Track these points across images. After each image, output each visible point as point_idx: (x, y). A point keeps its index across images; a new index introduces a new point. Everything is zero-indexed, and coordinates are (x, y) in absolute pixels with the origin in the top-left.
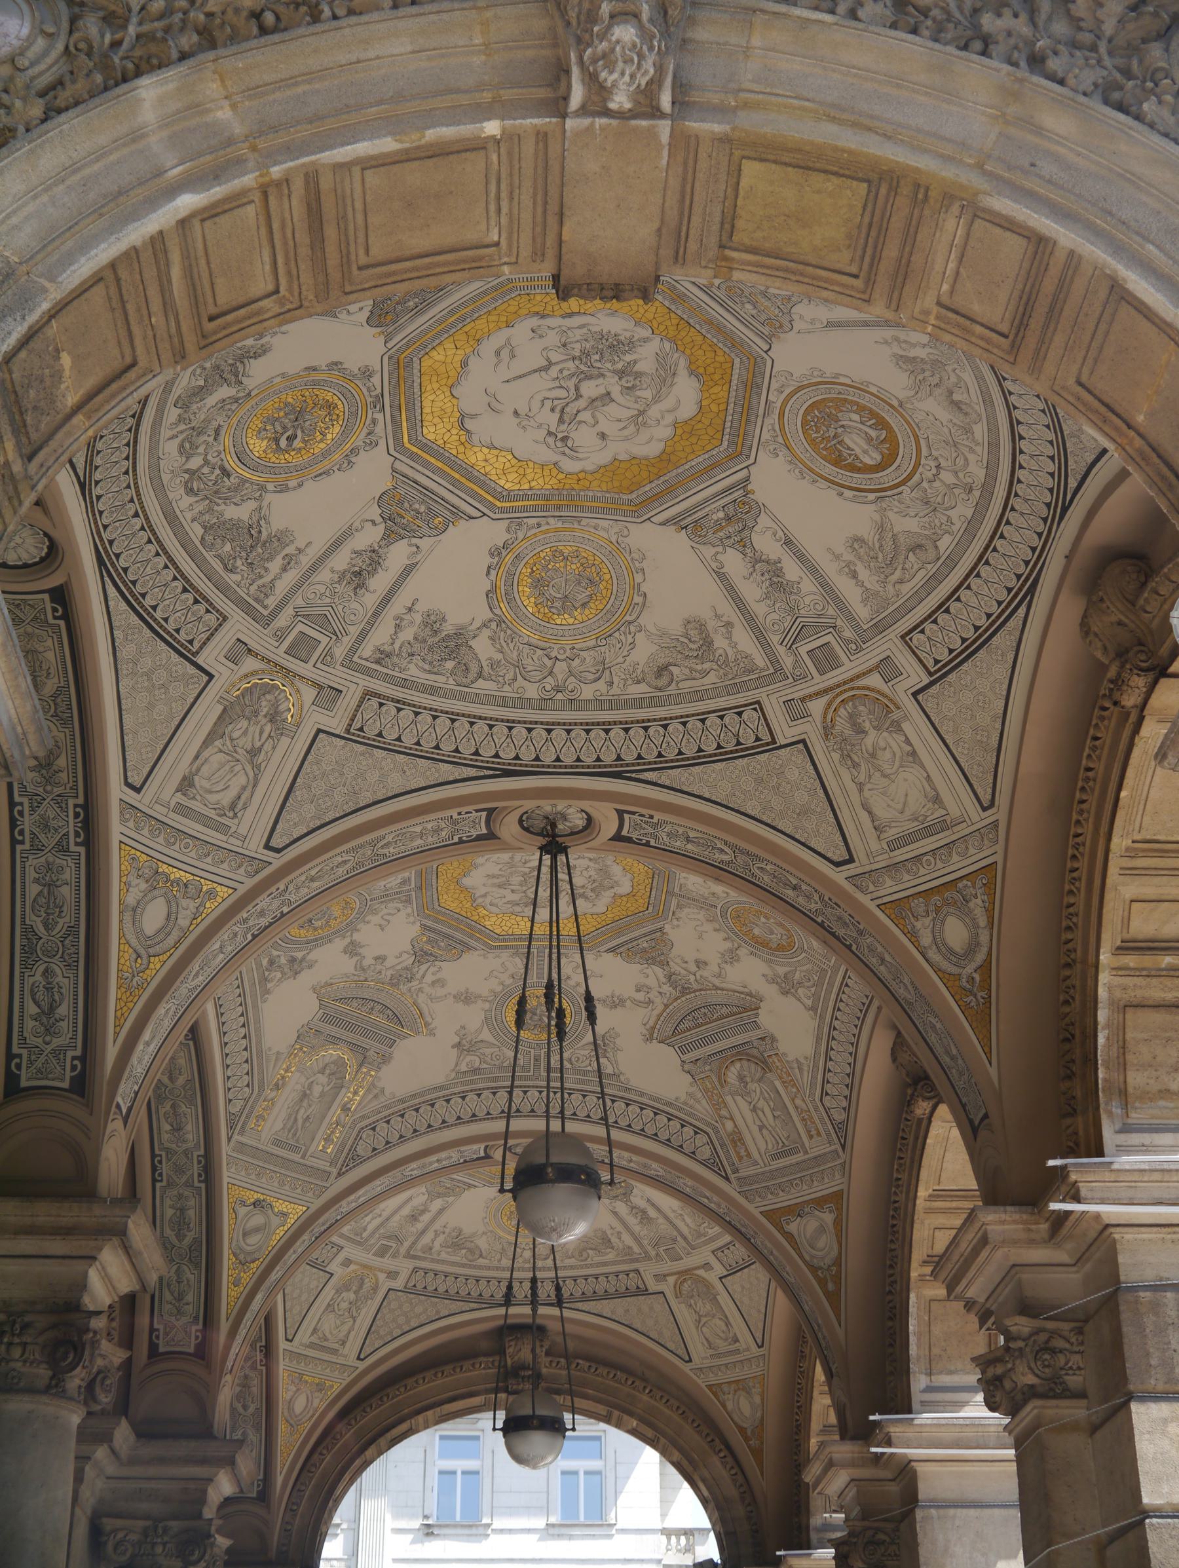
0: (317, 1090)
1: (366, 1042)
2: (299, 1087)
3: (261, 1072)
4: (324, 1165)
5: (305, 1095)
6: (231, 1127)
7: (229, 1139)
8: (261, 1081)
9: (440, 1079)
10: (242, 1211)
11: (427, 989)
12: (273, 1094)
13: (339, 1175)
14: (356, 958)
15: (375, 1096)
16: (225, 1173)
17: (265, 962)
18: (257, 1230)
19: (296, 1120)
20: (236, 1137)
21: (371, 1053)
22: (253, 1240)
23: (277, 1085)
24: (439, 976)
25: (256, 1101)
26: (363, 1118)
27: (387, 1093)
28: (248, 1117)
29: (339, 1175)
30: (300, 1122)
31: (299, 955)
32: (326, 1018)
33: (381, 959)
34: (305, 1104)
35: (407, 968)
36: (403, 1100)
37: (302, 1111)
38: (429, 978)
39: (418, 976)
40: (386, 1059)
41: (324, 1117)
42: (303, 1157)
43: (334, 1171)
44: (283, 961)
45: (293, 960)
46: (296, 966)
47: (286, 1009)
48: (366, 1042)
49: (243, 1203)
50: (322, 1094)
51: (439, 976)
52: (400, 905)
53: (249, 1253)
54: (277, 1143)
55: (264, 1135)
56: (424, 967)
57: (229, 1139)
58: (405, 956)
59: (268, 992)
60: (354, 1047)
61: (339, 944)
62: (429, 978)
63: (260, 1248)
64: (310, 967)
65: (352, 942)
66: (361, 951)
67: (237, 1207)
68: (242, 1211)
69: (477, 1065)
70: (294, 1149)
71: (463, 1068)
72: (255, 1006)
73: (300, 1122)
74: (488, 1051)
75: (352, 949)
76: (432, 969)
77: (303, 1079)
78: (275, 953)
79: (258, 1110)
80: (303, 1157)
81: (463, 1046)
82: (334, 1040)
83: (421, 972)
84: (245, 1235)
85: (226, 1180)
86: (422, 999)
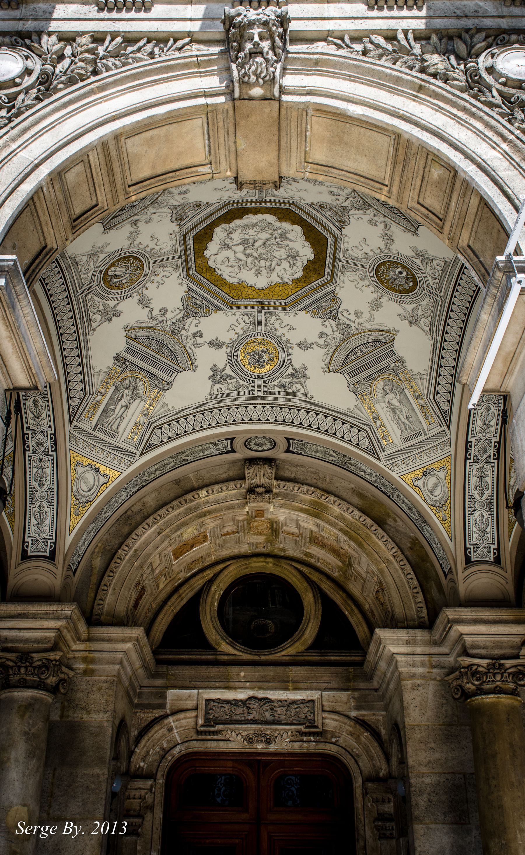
0: (395, 402)
1: (384, 364)
2: (386, 409)
3: (359, 420)
4: (438, 429)
5: (393, 409)
6: (373, 453)
7: (379, 459)
8: (364, 423)
9: (429, 345)
10: (420, 483)
11: (361, 321)
12: (378, 423)
13: (449, 427)
14: (315, 346)
15: (421, 379)
16: (393, 474)
17: (277, 389)
18: (436, 485)
19: (403, 423)
20: (381, 455)
21: (392, 366)
22: (437, 492)
23: (374, 418)
24: (352, 312)
25: (373, 433)
26: (428, 393)
27: (423, 372)
28: (378, 441)
29: (449, 427)
30: (406, 422)
31: (290, 371)
32: (352, 374)
33: (321, 336)
34: (398, 413)
35: (338, 325)
36: (432, 368)
37: (401, 417)
38: (352, 317)
39: (348, 321)
40: (400, 361)
41: (413, 410)
42: (426, 435)
43: (445, 428)
44: (288, 380)
45: (292, 375)
46: (300, 375)
47: (330, 390)
48: (384, 364)
49: (417, 479)
50: (400, 402)
51: (352, 312)
52: (274, 318)
53: (441, 499)
54: (407, 439)
55: (396, 442)
56: (340, 316)
57: (379, 459)
58: (327, 323)
59: (306, 395)
60: (383, 371)
61: (296, 352)
62: (352, 317)
63: (444, 492)
64: (306, 369)
65: (298, 345)
66: (309, 342)
67: (416, 483)
68: (420, 483)
69: (428, 322)
70: (418, 434)
71: (428, 329)
72: (310, 404)
73: (406, 422)
74: (420, 312)
75: (304, 346)
76: (345, 313)
77: (383, 405)
78: (276, 382)
79: (379, 435)
80: (426, 435)
81: (414, 321)
82: (370, 378)
83: (344, 319)
84: (431, 493)
85: (397, 477)
86: (368, 326)
